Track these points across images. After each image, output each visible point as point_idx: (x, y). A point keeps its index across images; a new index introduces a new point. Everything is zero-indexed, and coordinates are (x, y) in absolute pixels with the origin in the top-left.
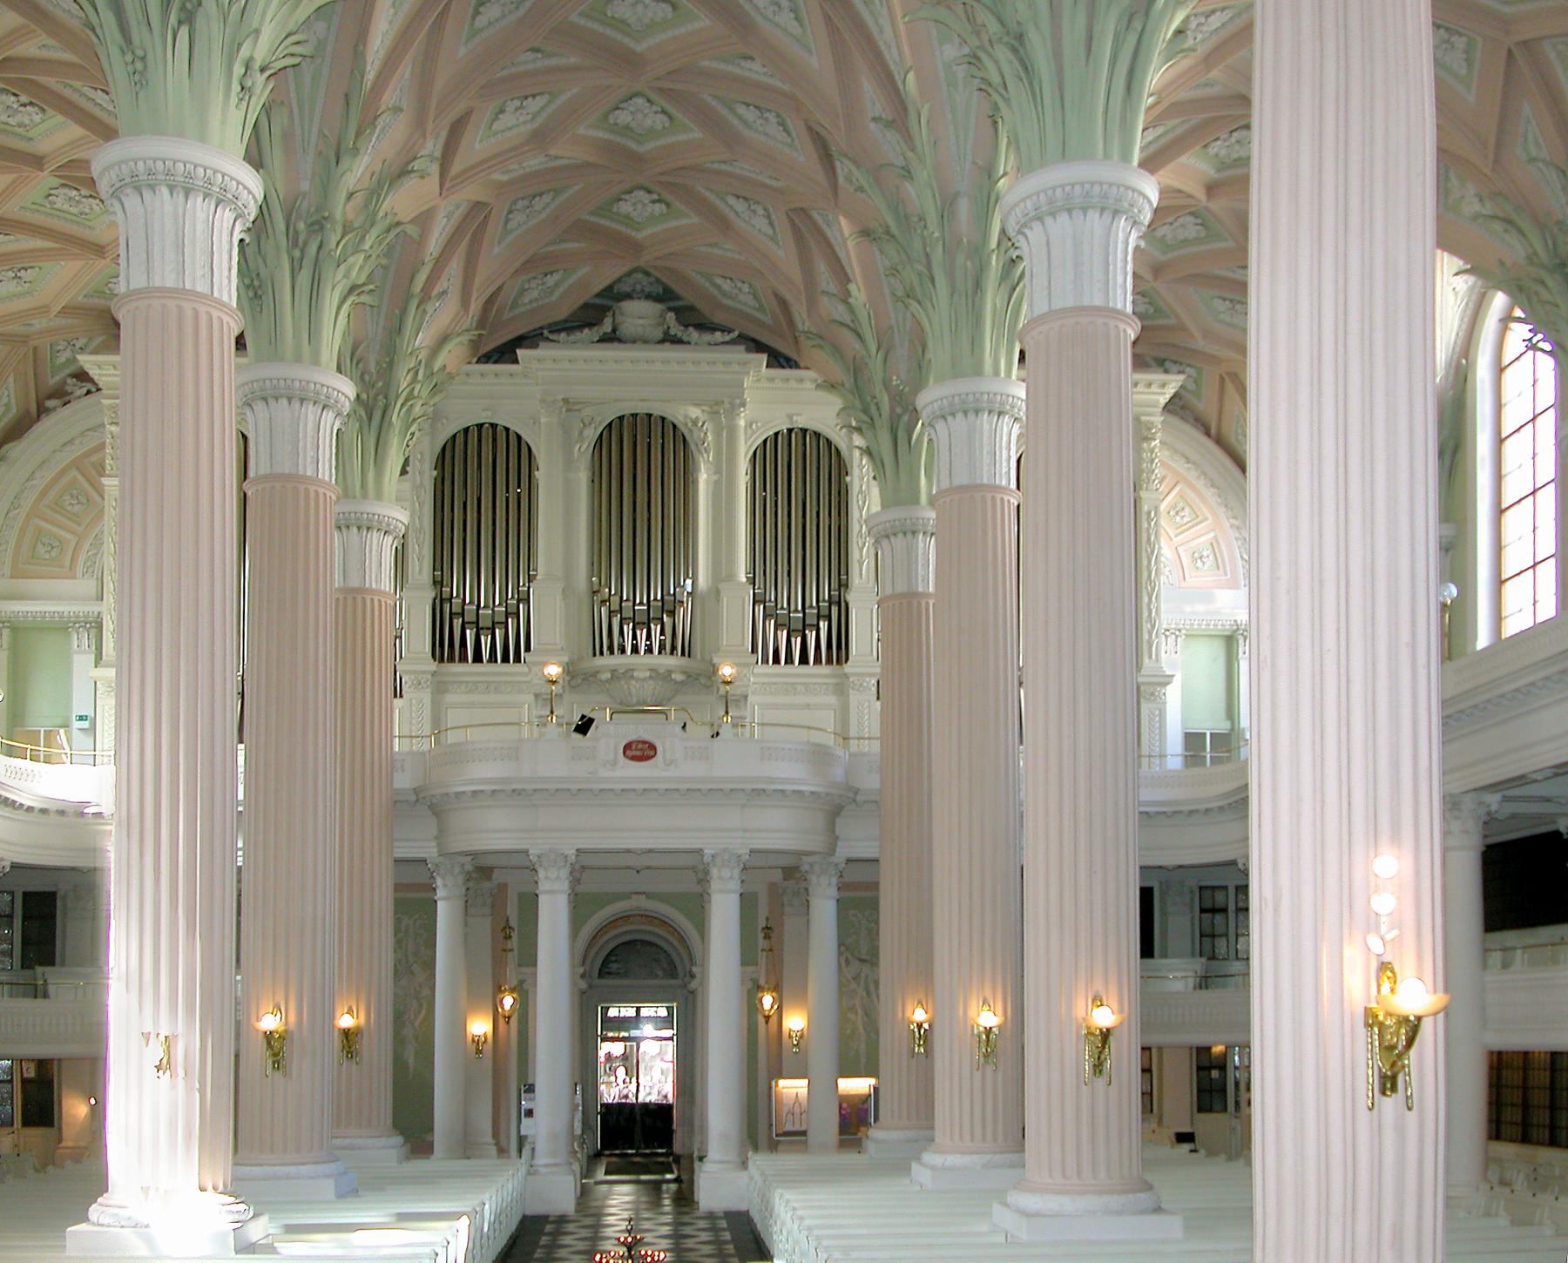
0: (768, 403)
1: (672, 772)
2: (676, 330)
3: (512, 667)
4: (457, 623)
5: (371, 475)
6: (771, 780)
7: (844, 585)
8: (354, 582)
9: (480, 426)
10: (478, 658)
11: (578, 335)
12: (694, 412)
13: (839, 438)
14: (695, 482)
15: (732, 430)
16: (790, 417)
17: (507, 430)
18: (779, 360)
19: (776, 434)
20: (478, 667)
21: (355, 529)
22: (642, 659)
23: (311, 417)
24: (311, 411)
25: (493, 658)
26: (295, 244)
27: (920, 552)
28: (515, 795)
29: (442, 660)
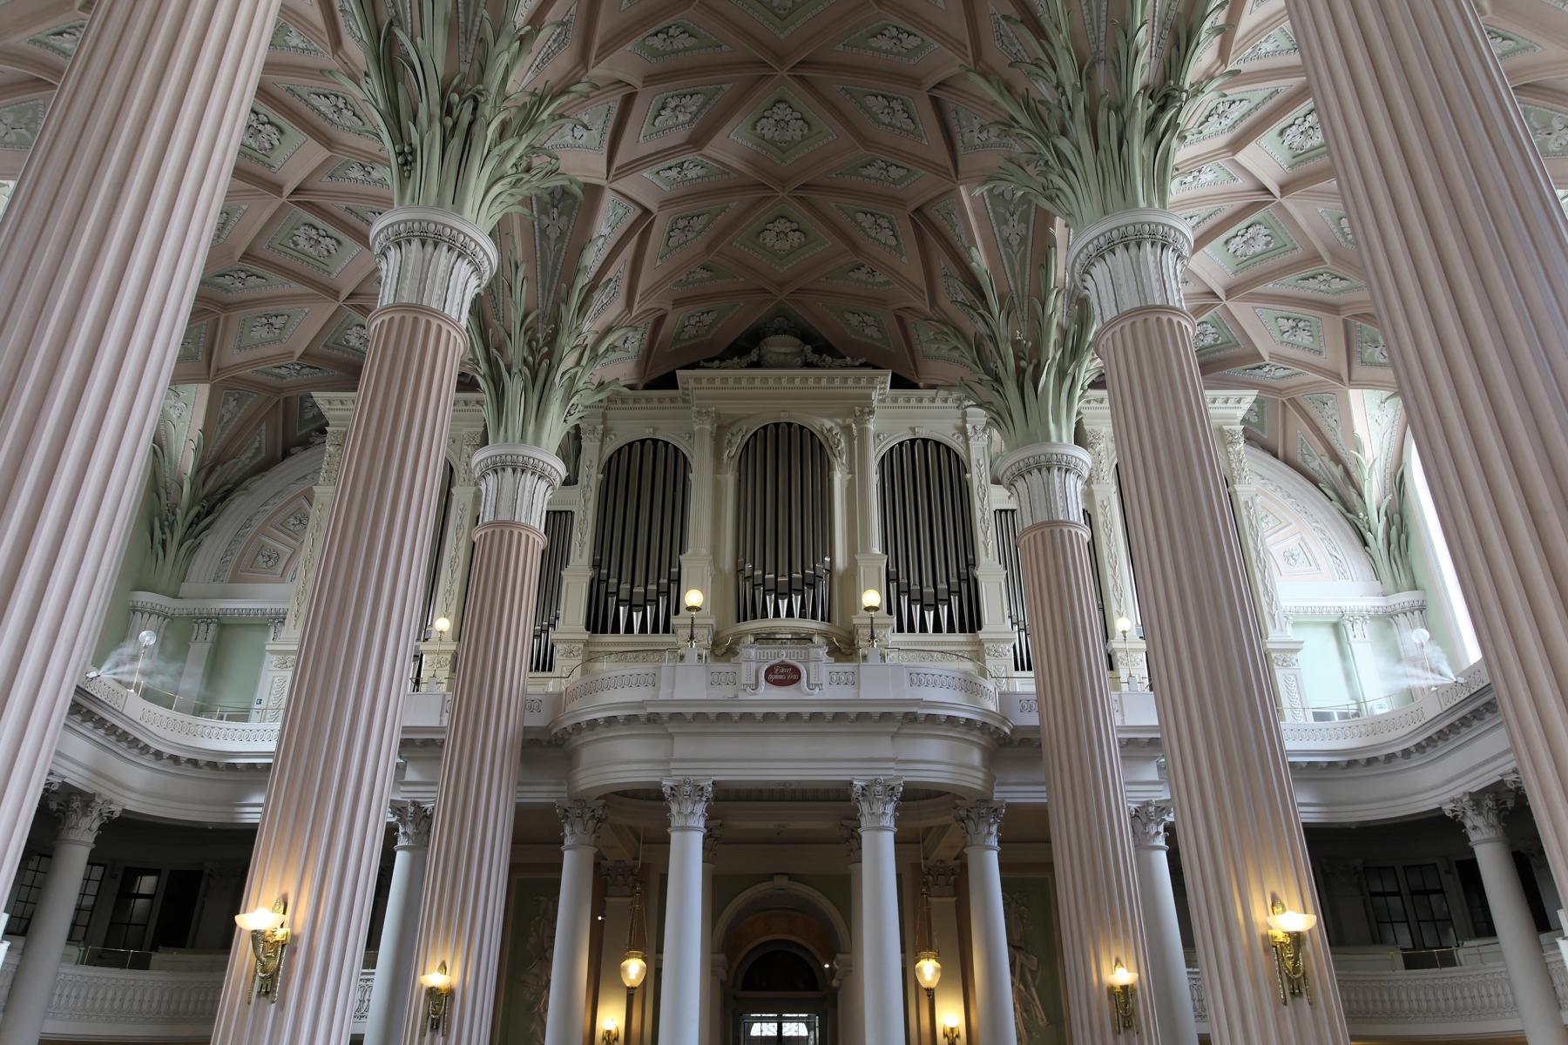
0: (892, 419)
1: (817, 694)
2: (814, 358)
3: (661, 638)
4: (612, 601)
5: (531, 428)
6: (918, 702)
7: (972, 564)
8: (504, 516)
9: (643, 442)
10: (629, 629)
11: (729, 362)
12: (828, 424)
13: (956, 444)
14: (831, 481)
15: (863, 432)
16: (913, 429)
17: (666, 444)
18: (898, 383)
19: (901, 444)
20: (629, 638)
21: (509, 470)
22: (784, 621)
23: (443, 261)
24: (443, 257)
25: (643, 629)
26: (449, 113)
27: (1057, 486)
28: (651, 721)
29: (595, 631)
